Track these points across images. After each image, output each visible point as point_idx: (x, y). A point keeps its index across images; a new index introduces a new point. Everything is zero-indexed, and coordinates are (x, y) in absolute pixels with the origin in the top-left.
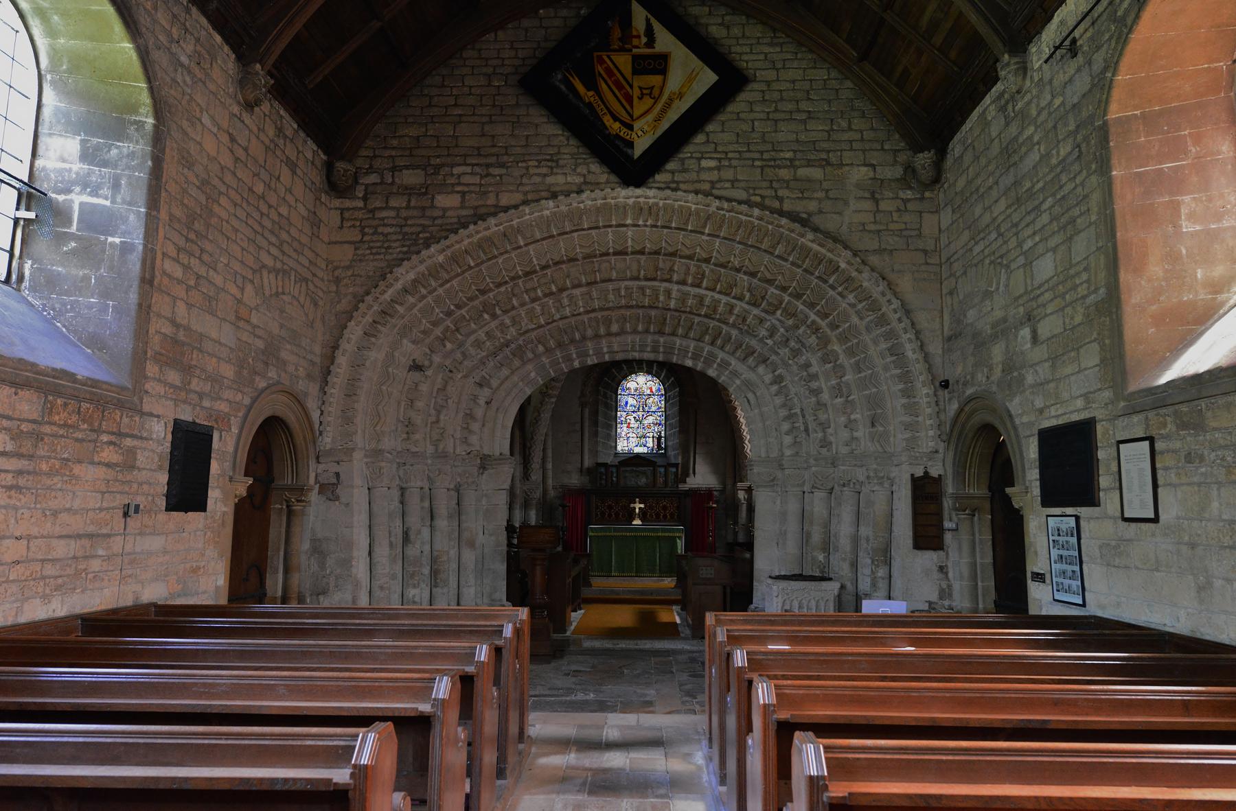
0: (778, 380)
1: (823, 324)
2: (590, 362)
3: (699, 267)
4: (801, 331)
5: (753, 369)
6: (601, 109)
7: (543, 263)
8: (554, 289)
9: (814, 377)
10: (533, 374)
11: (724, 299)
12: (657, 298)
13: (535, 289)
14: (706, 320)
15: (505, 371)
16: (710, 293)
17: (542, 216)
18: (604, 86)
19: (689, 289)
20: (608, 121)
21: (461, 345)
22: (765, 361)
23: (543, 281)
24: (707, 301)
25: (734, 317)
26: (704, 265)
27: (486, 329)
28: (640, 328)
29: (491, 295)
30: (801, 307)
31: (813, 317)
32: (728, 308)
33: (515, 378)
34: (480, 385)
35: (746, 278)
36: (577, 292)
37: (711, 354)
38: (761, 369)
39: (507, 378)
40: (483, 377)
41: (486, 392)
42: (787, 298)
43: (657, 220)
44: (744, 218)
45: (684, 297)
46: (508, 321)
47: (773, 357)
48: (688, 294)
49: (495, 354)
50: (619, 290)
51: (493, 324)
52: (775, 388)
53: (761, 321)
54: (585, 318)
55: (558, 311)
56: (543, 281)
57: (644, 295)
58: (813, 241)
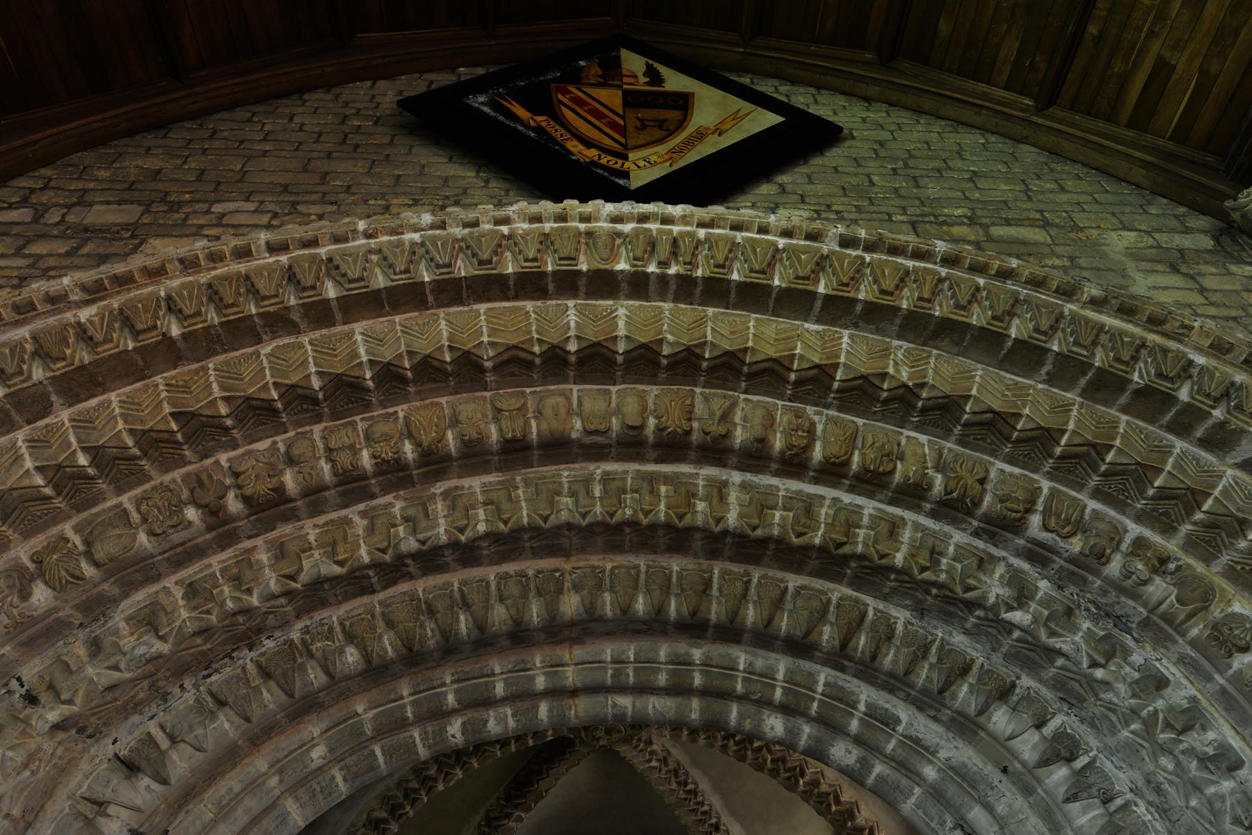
0: (1062, 749)
1: (1171, 546)
2: (493, 727)
3: (798, 415)
4: (1114, 567)
5: (966, 726)
6: (558, 132)
7: (387, 355)
8: (408, 451)
9: (1191, 719)
10: (318, 754)
11: (869, 507)
12: (691, 506)
13: (354, 450)
14: (818, 584)
15: (226, 725)
16: (829, 493)
17: (400, 244)
18: (567, 113)
19: (775, 481)
20: (574, 146)
21: (96, 608)
22: (1004, 693)
23: (381, 428)
24: (824, 513)
25: (904, 548)
26: (810, 410)
27: (186, 573)
28: (641, 605)
29: (224, 458)
30: (1093, 505)
31: (1134, 529)
32: (884, 528)
33: (260, 763)
34: (130, 767)
35: (923, 438)
36: (475, 484)
37: (838, 695)
38: (1000, 719)
39: (230, 757)
40: (150, 740)
41: (144, 791)
42: (1046, 485)
43: (692, 264)
44: (910, 264)
45: (762, 504)
46: (264, 557)
47: (1026, 681)
48: (771, 491)
49: (206, 663)
50: (588, 481)
51: (216, 561)
52: (1059, 774)
53: (984, 562)
54: (490, 573)
55: (414, 531)
56: (381, 428)
57: (654, 492)
58: (1096, 303)
